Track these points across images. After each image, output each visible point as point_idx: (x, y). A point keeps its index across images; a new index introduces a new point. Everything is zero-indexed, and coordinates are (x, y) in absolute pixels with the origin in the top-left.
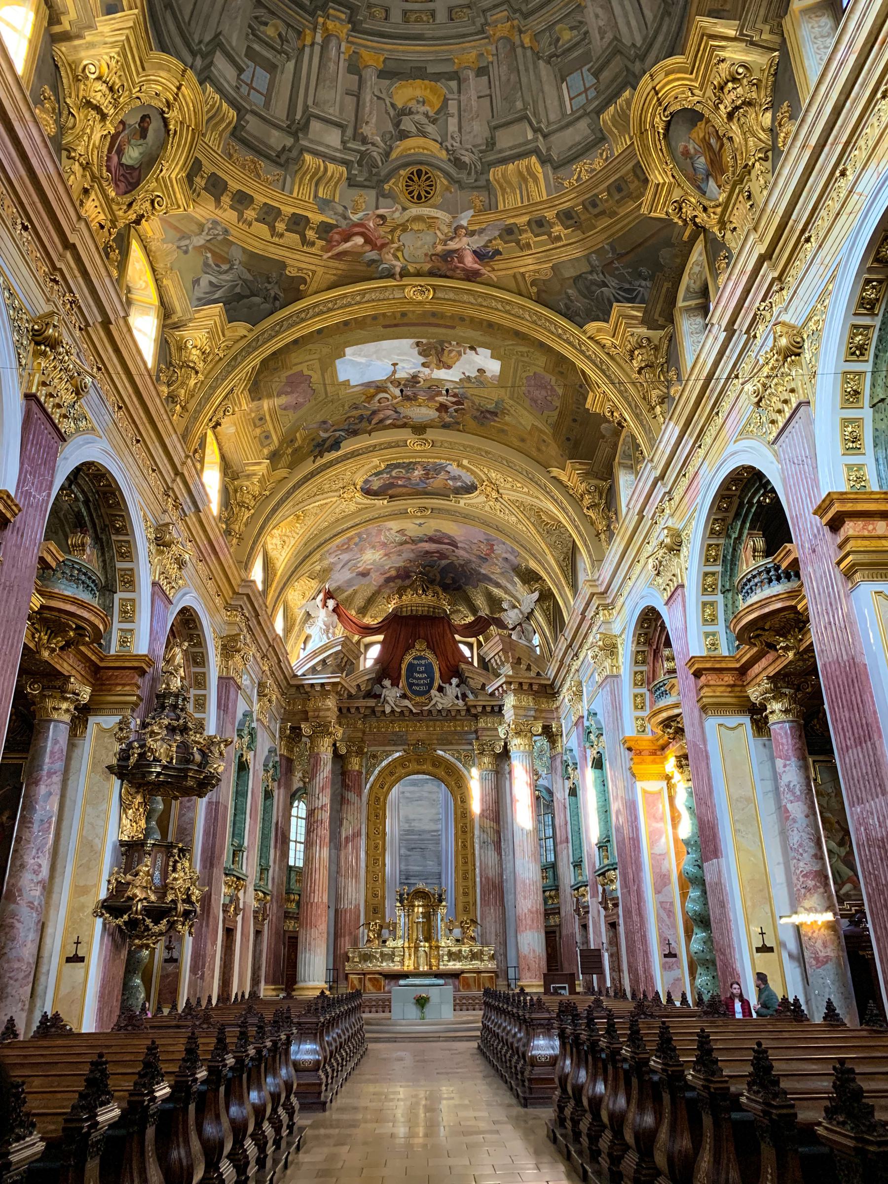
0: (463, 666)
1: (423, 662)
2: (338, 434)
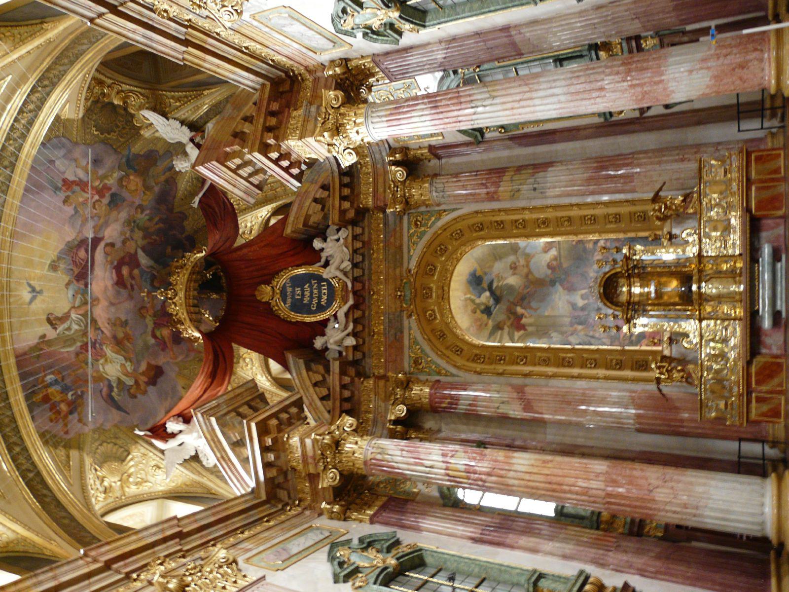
0: (288, 230)
1: (289, 290)
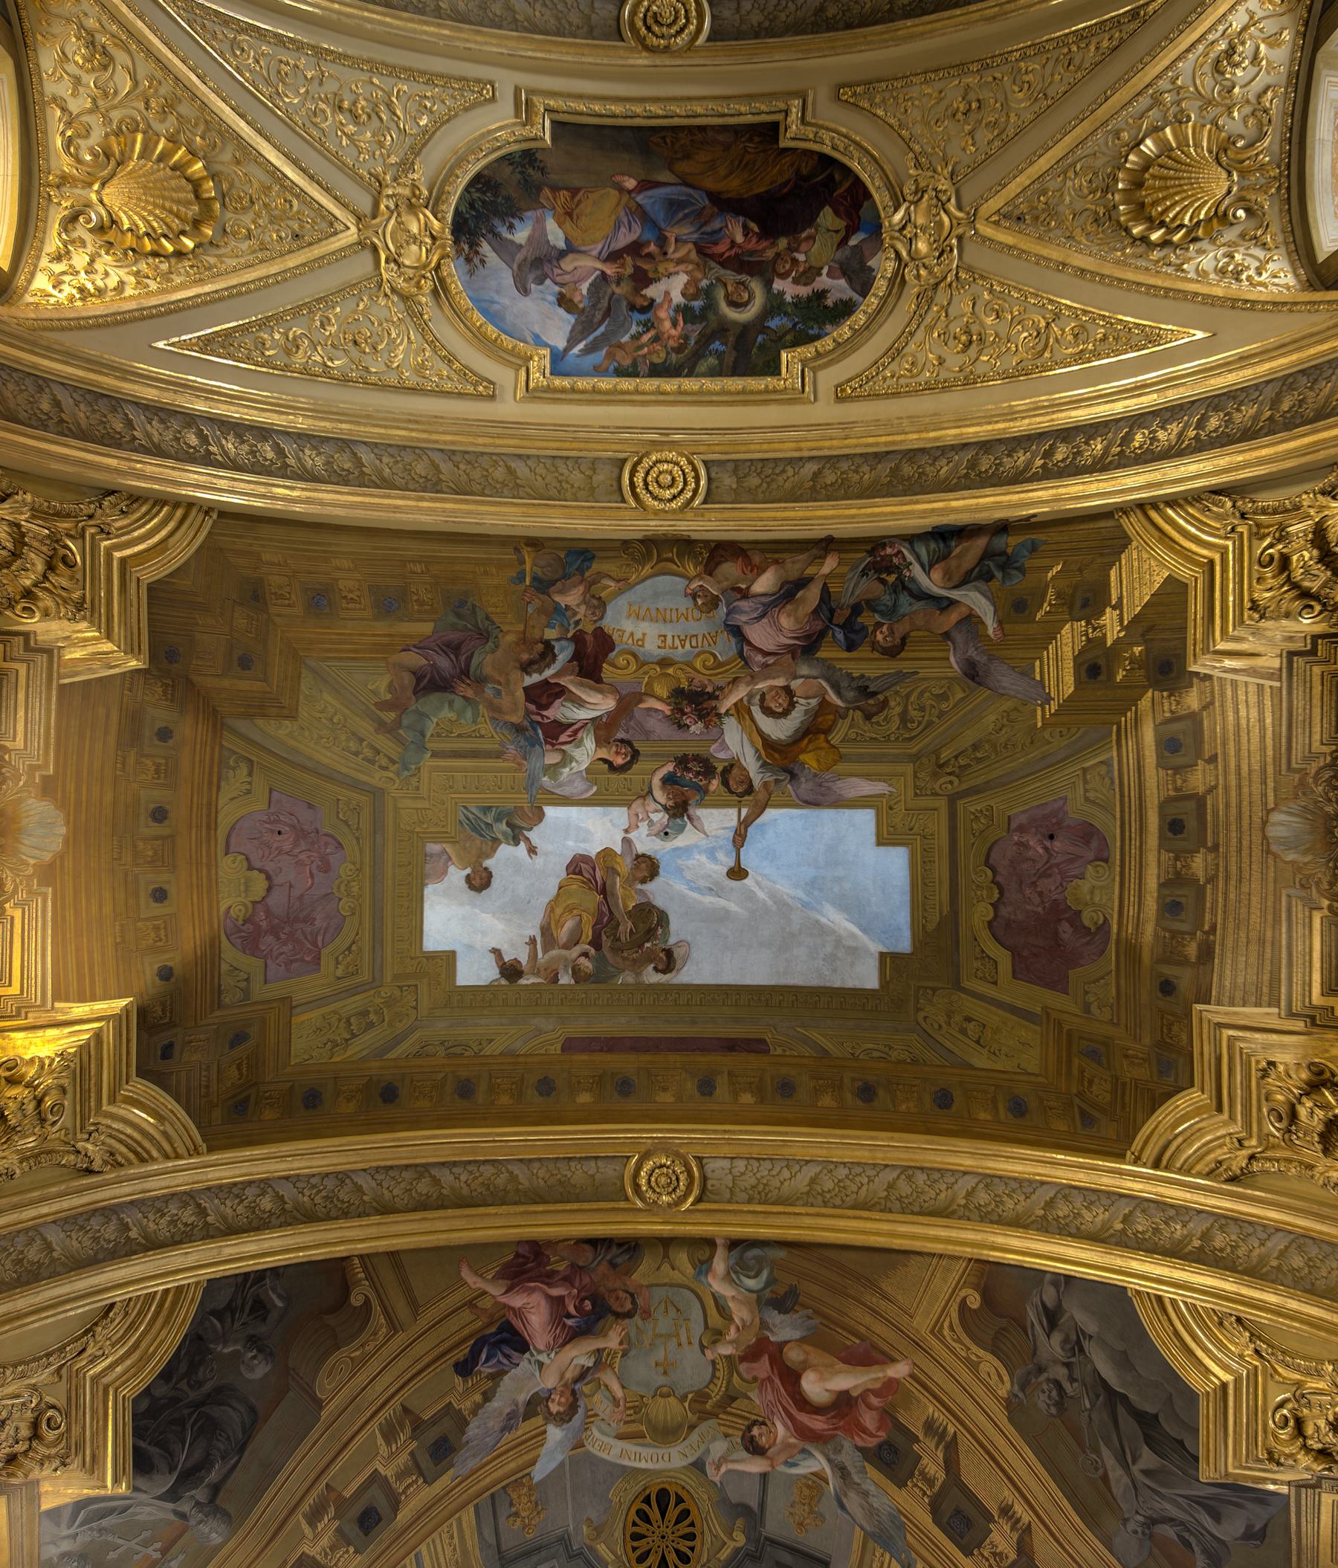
2: (931, 582)
